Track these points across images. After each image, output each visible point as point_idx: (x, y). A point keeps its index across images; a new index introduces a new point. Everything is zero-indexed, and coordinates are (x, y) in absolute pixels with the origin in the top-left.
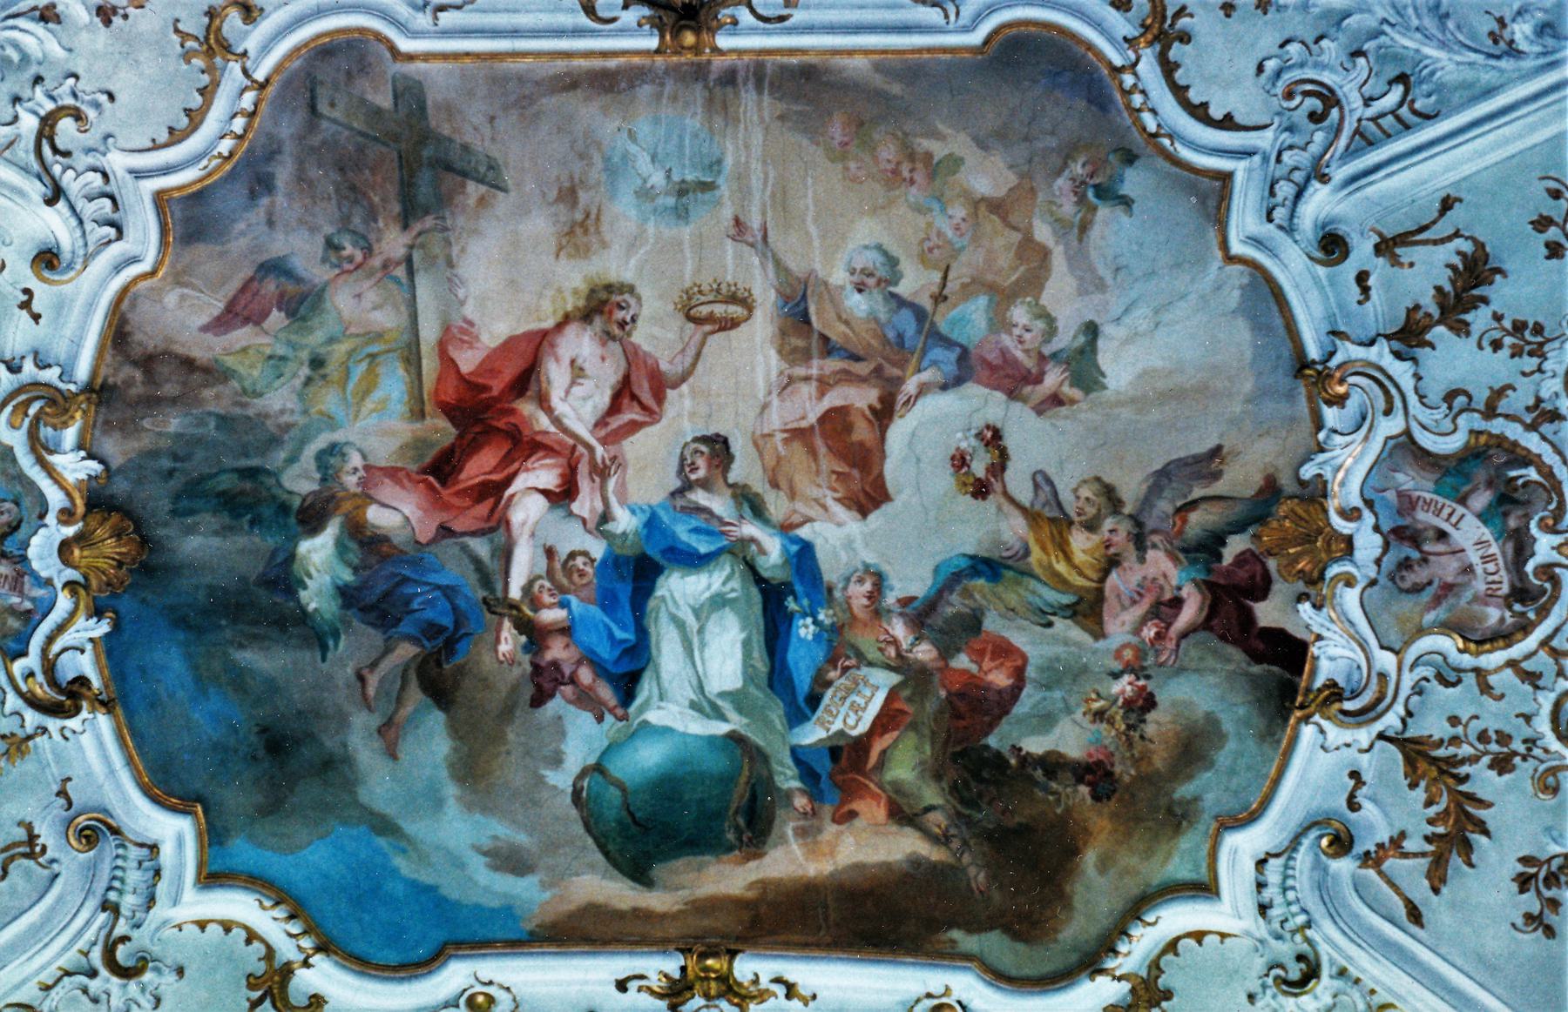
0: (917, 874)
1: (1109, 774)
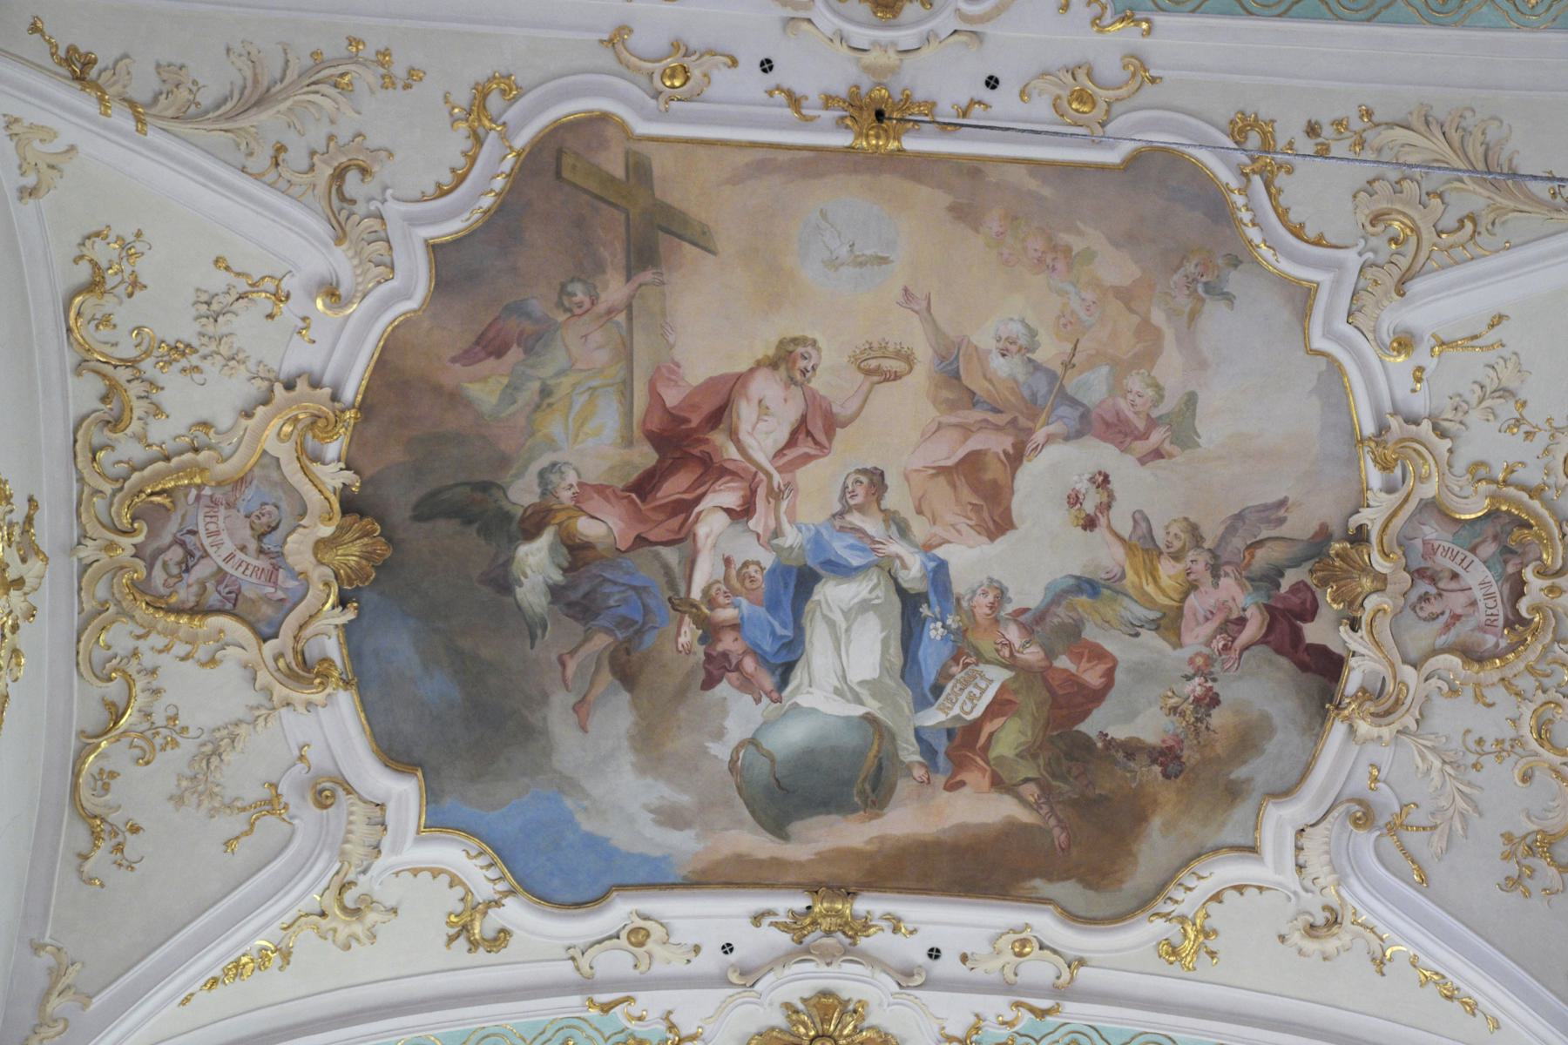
0: (1011, 832)
1: (1178, 758)
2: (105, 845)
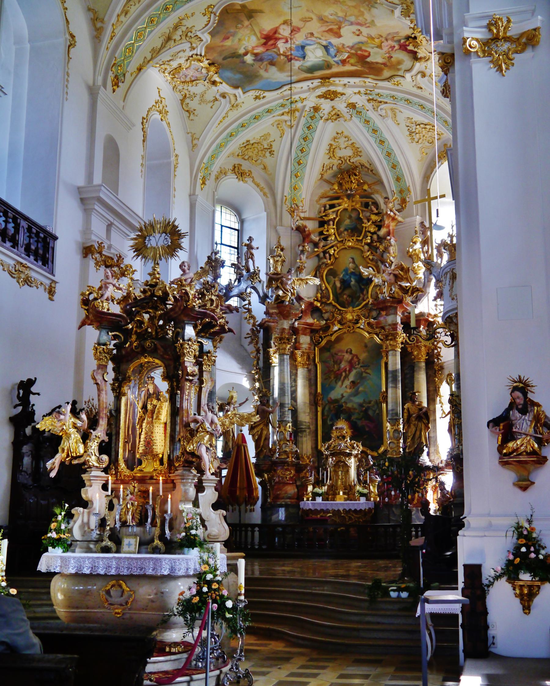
2: (192, 114)
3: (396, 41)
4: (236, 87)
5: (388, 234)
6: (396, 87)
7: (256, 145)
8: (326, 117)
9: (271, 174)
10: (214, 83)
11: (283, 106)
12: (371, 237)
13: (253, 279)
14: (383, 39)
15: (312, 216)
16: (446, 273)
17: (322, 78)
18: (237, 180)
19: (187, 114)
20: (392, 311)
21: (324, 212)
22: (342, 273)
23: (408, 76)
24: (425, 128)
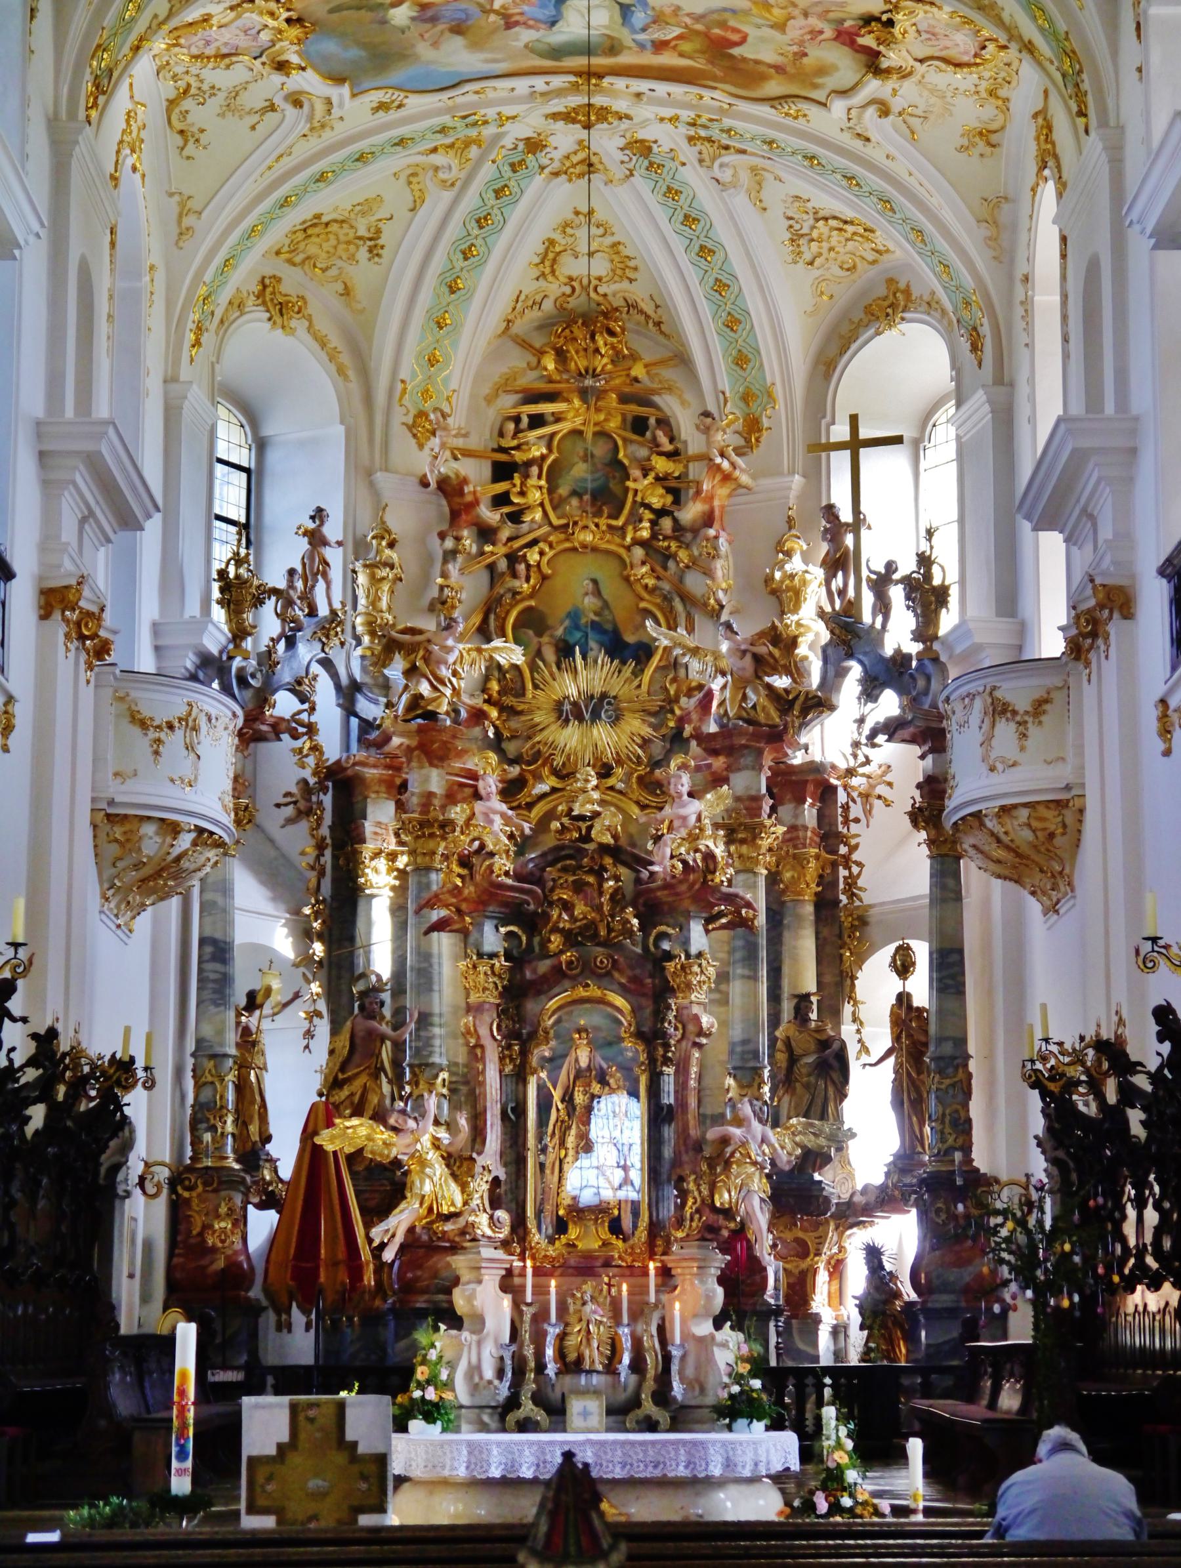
2: (192, 140)
3: (829, 21)
4: (339, 80)
5: (708, 520)
6: (789, 121)
7: (334, 227)
8: (556, 166)
9: (362, 311)
10: (282, 66)
11: (443, 130)
12: (654, 523)
13: (328, 637)
14: (796, 12)
15: (473, 443)
16: (972, 696)
17: (578, 74)
18: (268, 325)
19: (179, 140)
20: (748, 760)
21: (514, 436)
22: (562, 623)
23: (839, 106)
24: (840, 230)
